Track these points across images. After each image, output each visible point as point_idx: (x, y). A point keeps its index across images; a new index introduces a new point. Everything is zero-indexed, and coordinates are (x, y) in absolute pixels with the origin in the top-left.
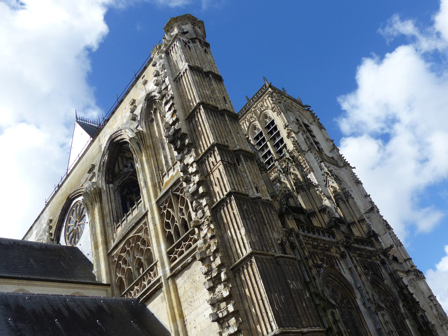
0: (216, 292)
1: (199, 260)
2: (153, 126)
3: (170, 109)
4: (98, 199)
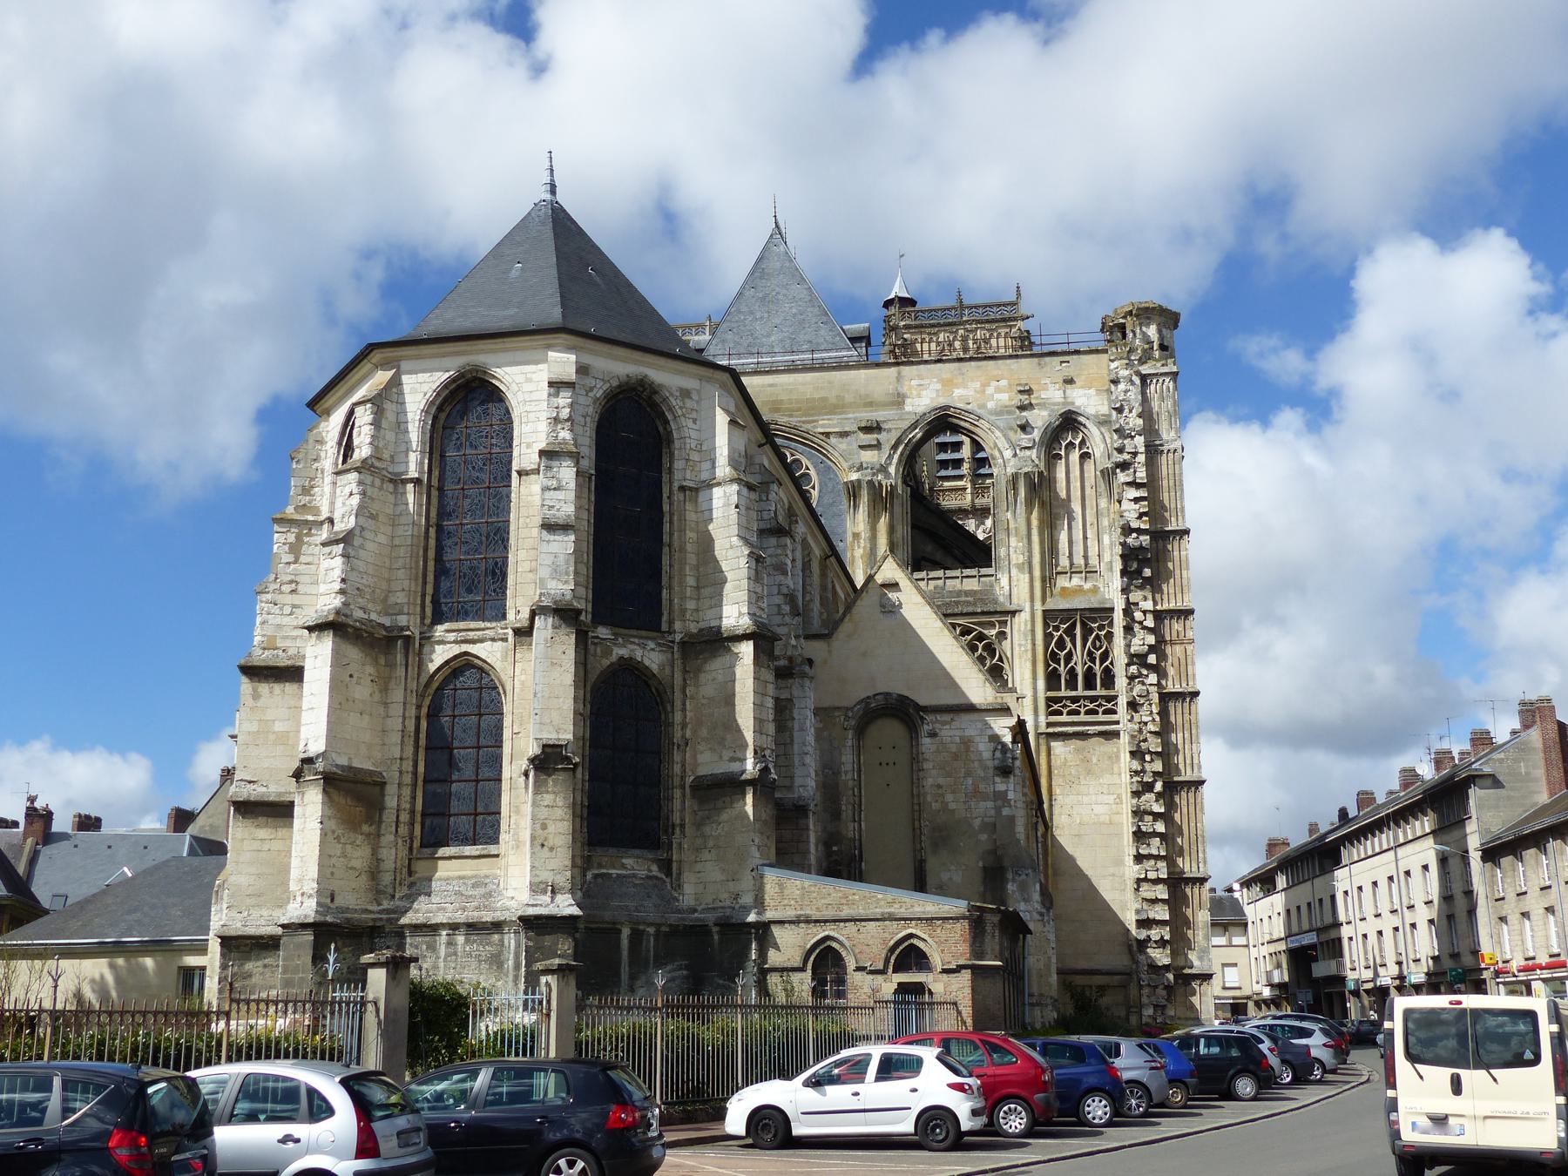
2: (1055, 466)
3: (1136, 500)
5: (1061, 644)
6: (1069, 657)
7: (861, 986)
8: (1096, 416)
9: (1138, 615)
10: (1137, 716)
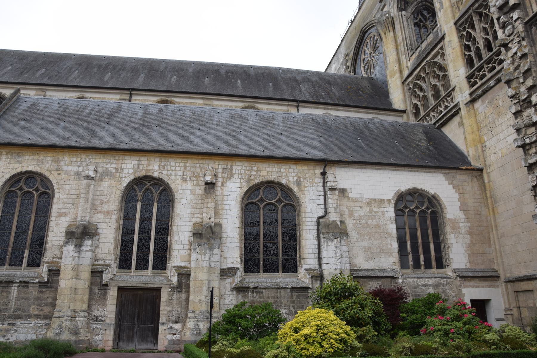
0: (524, 116)
1: (505, 83)
4: (391, 28)
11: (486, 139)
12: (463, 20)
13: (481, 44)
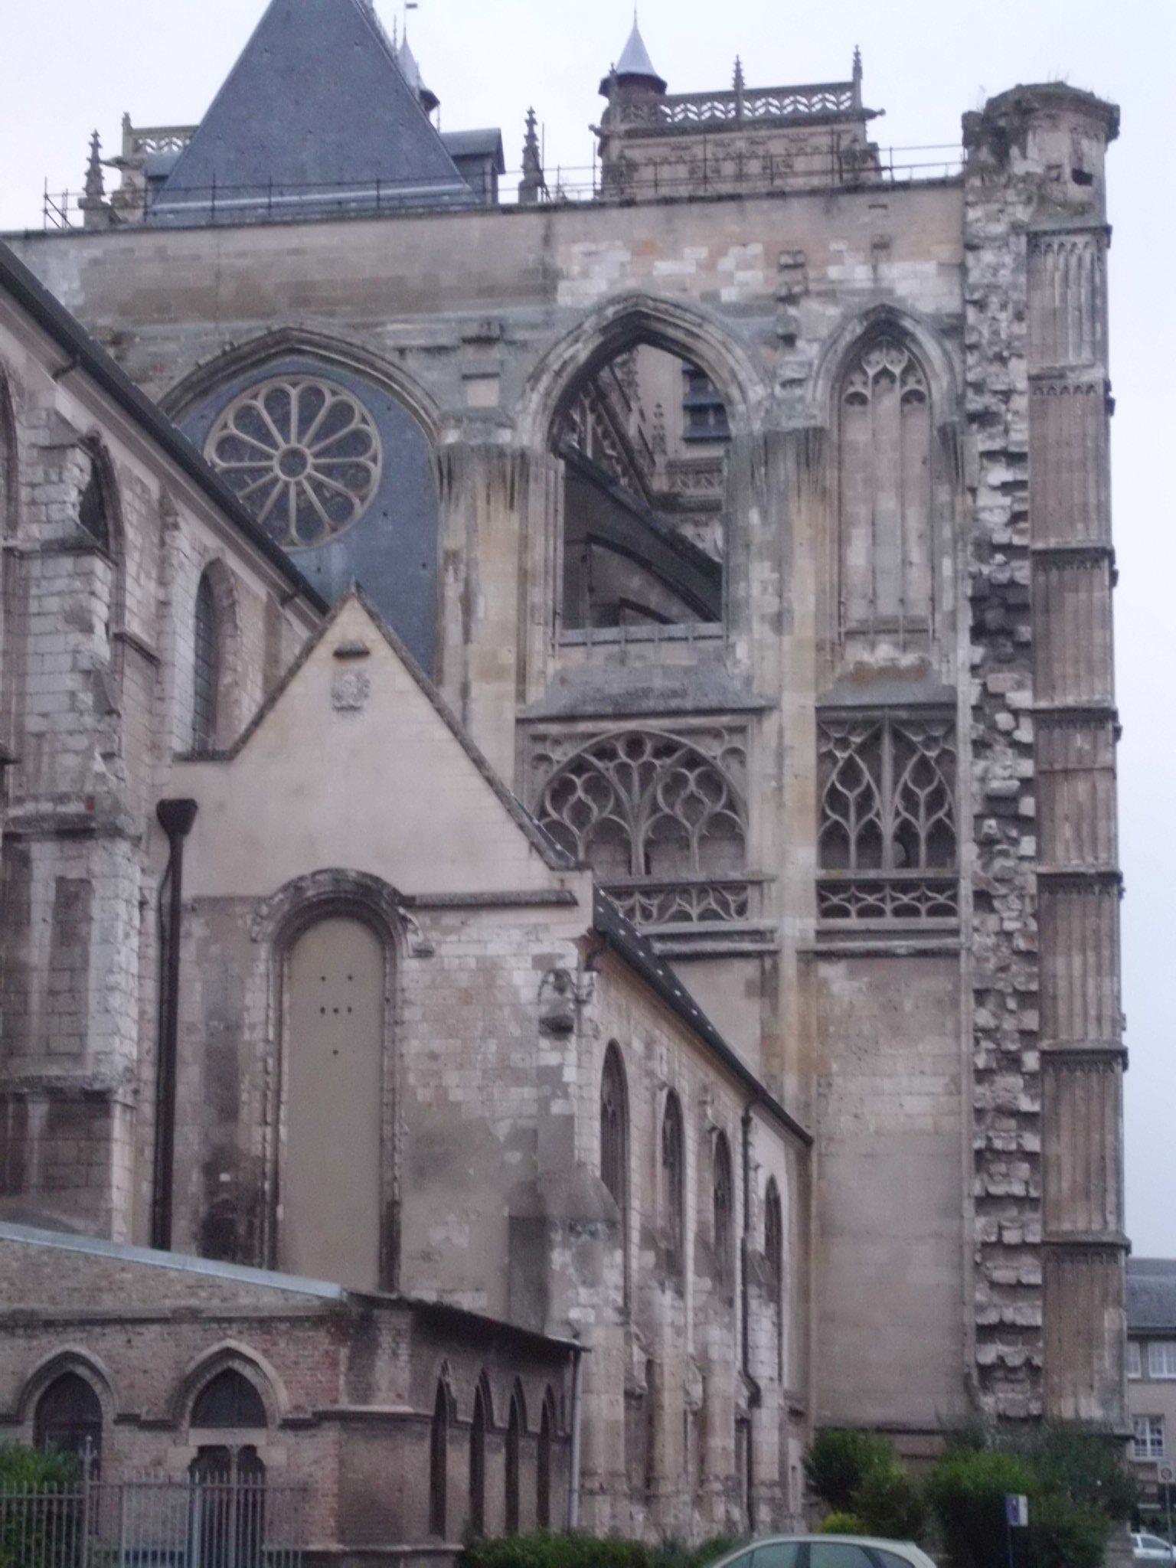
3: (1006, 488)
5: (850, 775)
6: (866, 798)
7: (131, 1453)
8: (936, 318)
9: (1003, 719)
10: (992, 922)
11: (835, 1067)
12: (844, 714)
13: (888, 827)
